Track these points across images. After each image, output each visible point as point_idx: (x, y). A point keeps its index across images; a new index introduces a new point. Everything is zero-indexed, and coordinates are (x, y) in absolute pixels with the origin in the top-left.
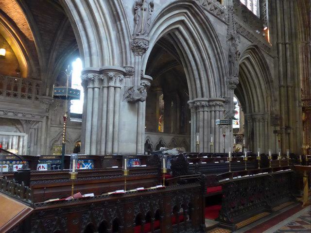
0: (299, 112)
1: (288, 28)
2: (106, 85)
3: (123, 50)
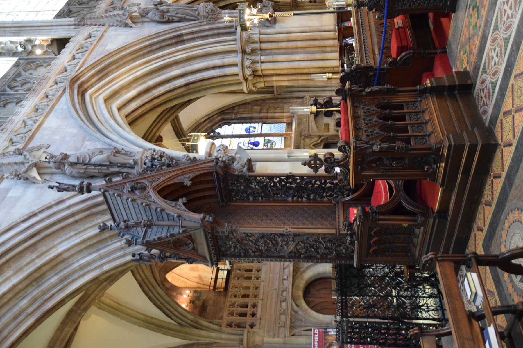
2: (257, 46)
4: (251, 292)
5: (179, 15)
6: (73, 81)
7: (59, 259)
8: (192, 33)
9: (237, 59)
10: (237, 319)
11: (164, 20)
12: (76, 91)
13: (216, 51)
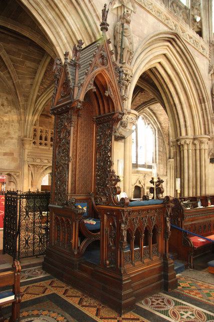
4: (43, 141)
6: (176, 35)
7: (63, 19)
8: (206, 109)
9: (191, 134)
10: (39, 134)
12: (170, 36)
13: (195, 122)
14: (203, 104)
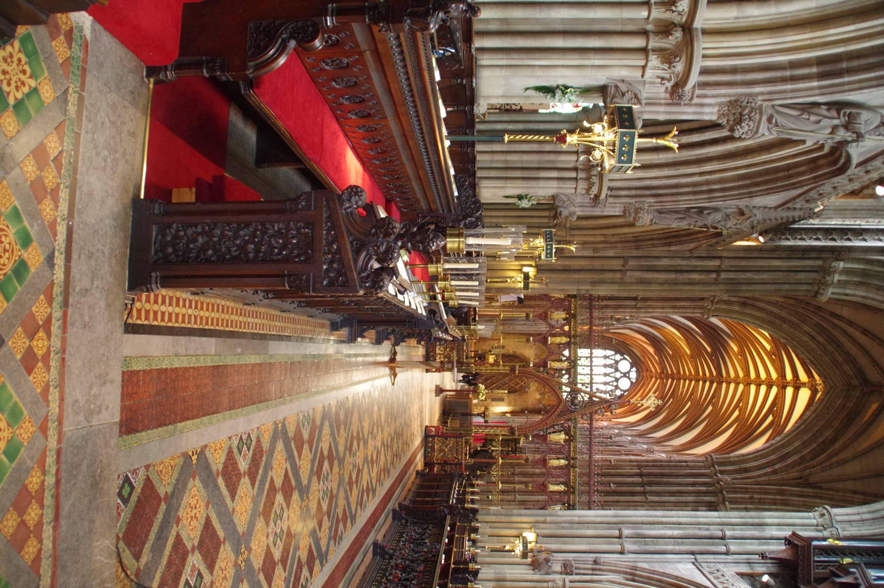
0: (566, 290)
1: (752, 279)
3: (739, 77)
5: (813, 118)
8: (793, 79)
11: (848, 111)
13: (753, 36)
14: (814, 70)
